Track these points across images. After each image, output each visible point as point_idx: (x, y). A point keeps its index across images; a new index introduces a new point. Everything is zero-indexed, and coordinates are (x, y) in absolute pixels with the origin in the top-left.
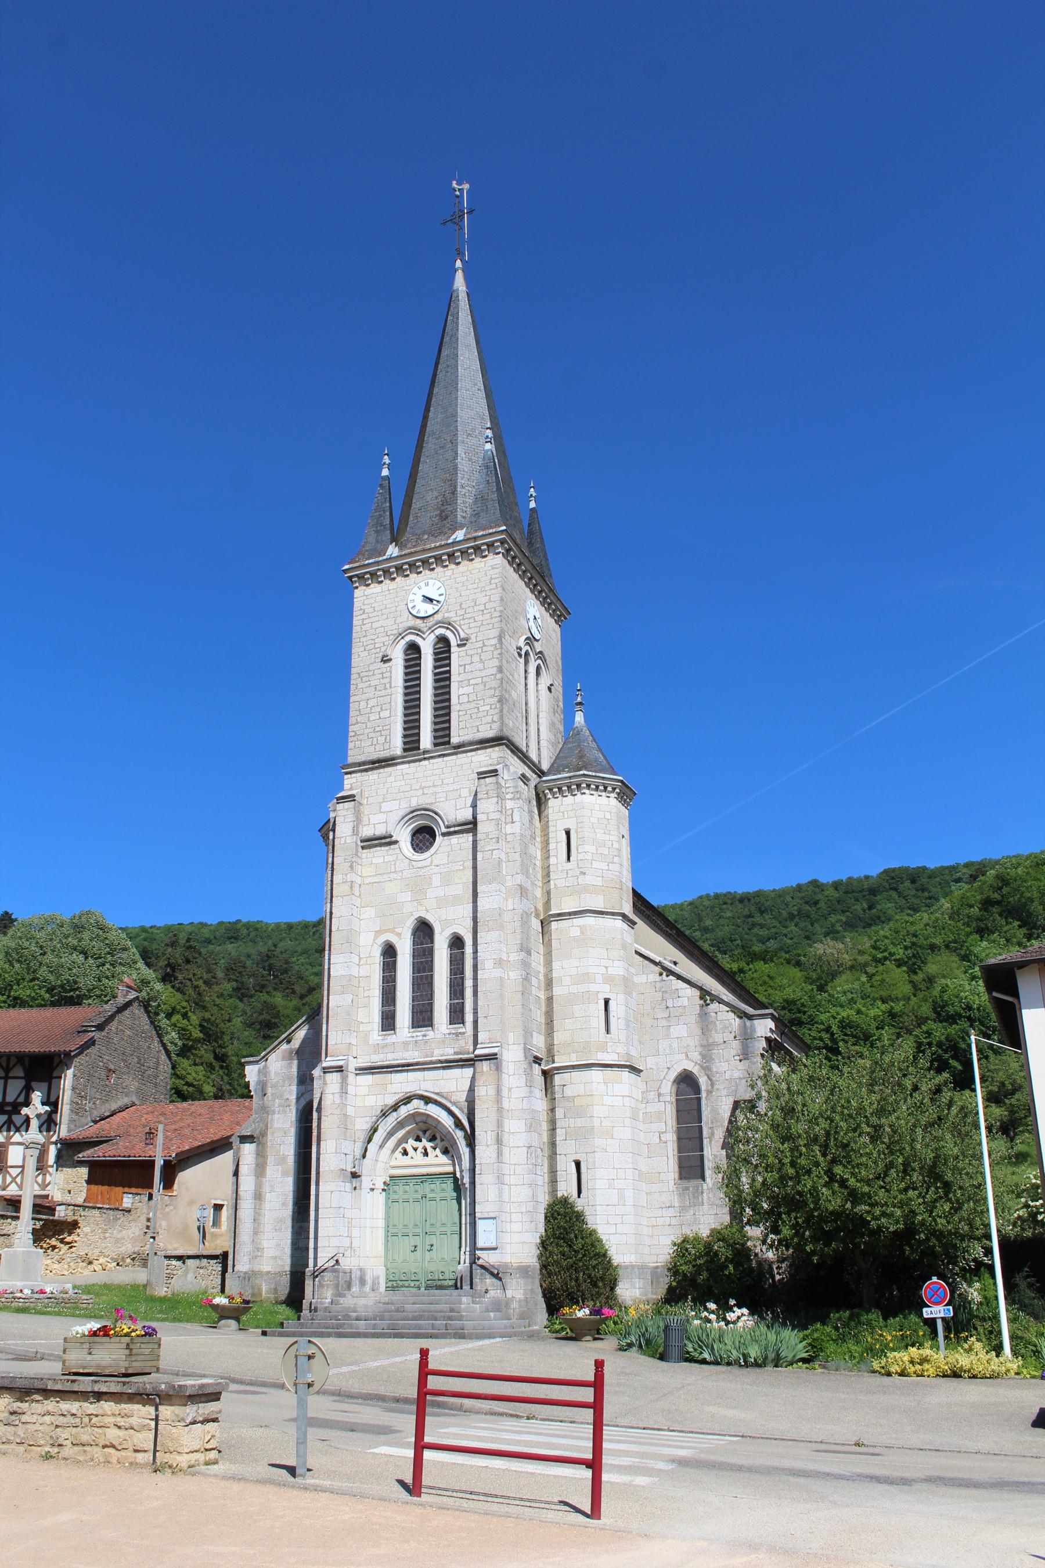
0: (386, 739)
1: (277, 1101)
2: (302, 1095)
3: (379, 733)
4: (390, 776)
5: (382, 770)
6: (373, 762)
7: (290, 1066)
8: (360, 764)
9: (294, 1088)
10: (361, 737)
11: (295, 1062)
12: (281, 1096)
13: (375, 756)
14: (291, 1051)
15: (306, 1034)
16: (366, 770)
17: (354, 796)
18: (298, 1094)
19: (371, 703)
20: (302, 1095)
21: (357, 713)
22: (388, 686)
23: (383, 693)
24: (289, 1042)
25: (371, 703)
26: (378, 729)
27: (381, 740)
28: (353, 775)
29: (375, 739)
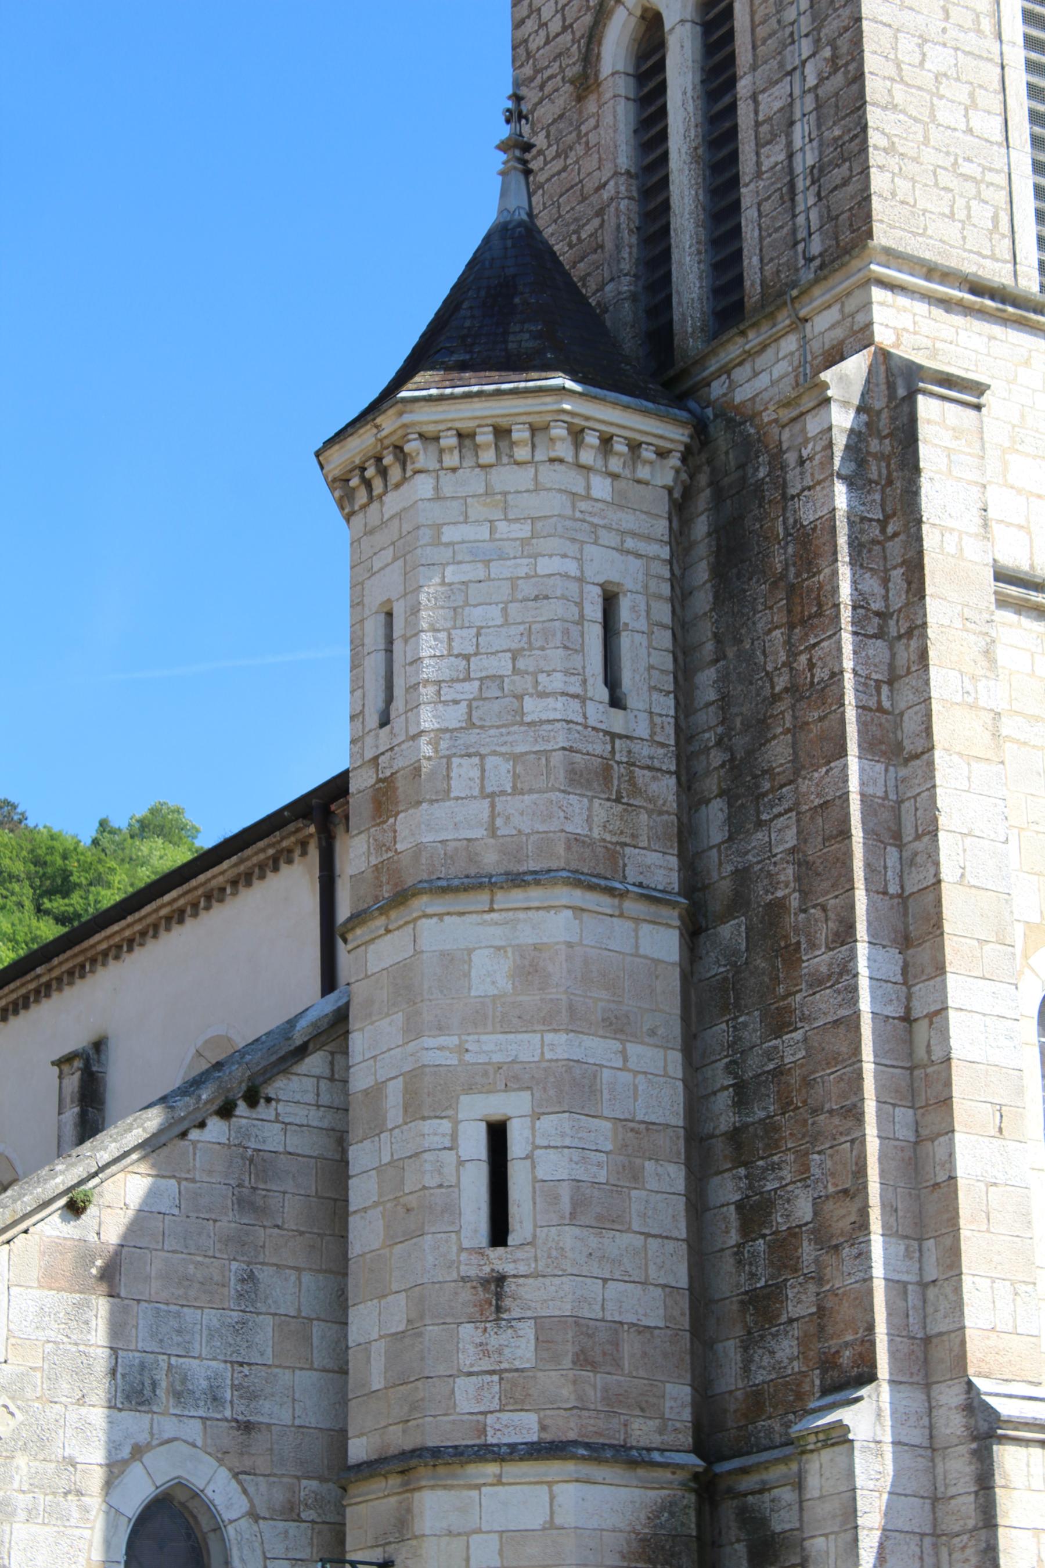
0: (995, 219)
1: (21, 1461)
2: (138, 1452)
3: (970, 188)
4: (1027, 363)
5: (997, 330)
6: (977, 288)
7: (78, 1315)
8: (931, 271)
9: (97, 1415)
10: (911, 168)
11: (101, 1307)
12: (42, 1442)
13: (970, 266)
14: (84, 1255)
15: (152, 1194)
16: (946, 304)
17: (979, 388)
18: (113, 1446)
19: (939, 59)
20: (138, 1452)
21: (891, 70)
22: (987, 25)
23: (970, 43)
24: (75, 1208)
25: (939, 59)
26: (966, 168)
27: (982, 215)
28: (902, 301)
29: (960, 203)
